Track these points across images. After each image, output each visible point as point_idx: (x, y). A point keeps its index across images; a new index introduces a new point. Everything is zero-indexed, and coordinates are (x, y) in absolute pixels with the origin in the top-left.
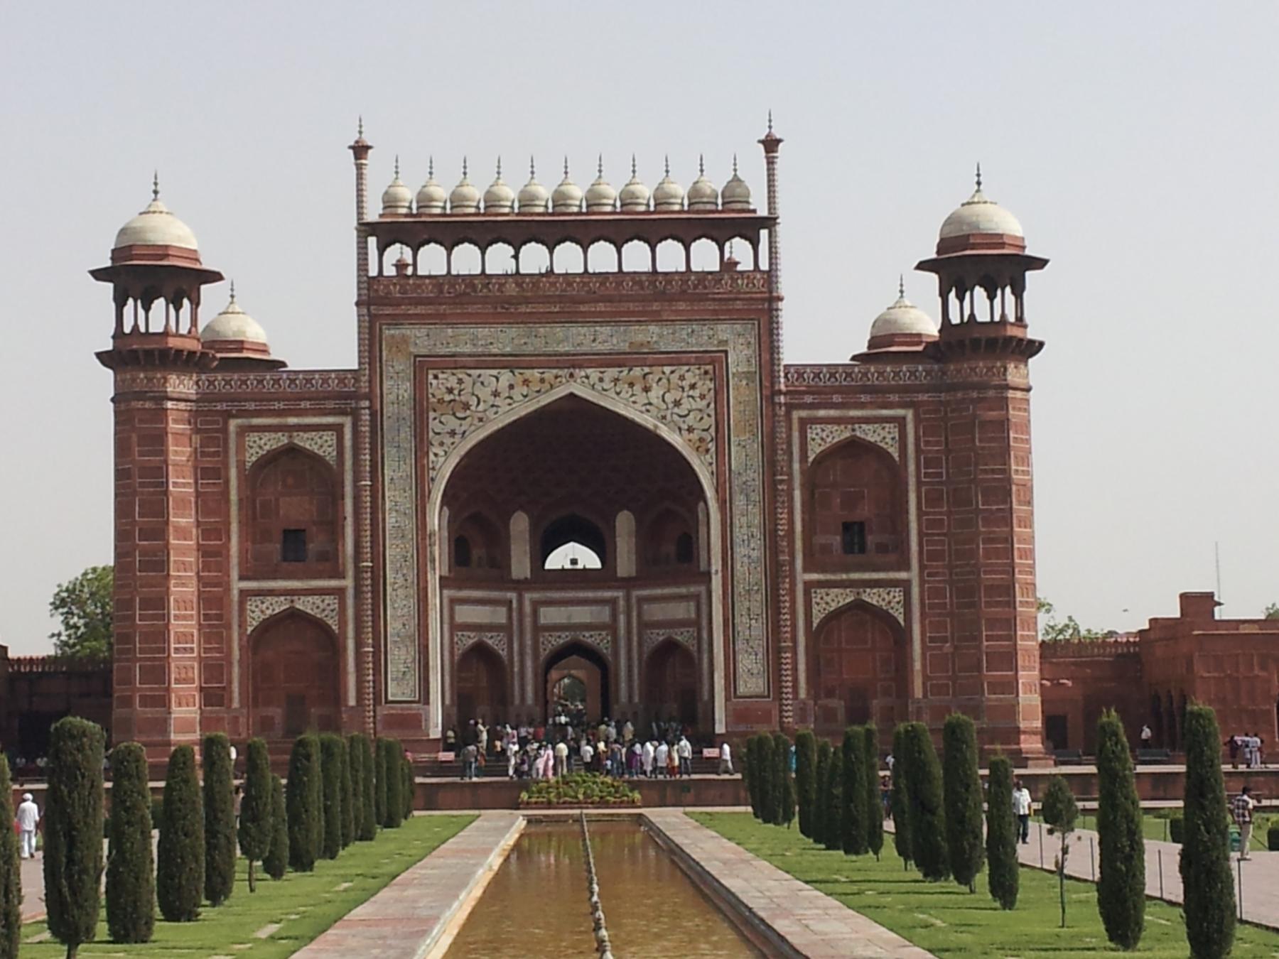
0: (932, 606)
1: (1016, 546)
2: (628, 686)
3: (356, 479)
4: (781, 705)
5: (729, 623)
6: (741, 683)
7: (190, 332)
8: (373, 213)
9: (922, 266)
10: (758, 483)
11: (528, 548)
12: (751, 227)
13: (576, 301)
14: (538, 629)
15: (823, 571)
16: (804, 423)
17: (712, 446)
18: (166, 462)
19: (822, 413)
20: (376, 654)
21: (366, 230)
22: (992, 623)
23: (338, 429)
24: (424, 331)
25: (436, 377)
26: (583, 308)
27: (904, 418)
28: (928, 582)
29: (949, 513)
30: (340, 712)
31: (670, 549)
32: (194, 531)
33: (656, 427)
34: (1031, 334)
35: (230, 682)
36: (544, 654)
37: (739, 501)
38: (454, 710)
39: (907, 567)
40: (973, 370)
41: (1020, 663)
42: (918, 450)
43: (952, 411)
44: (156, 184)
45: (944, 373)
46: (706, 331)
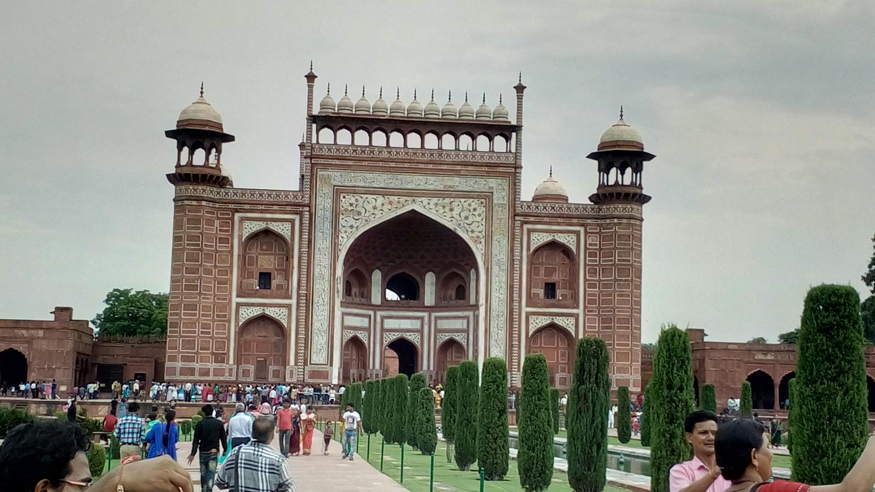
0: (589, 327)
3: (300, 249)
5: (487, 331)
8: (316, 112)
9: (592, 156)
10: (505, 260)
12: (507, 130)
16: (529, 231)
17: (483, 240)
20: (306, 339)
22: (621, 336)
23: (292, 222)
24: (338, 174)
26: (421, 166)
27: (579, 232)
31: (452, 293)
34: (645, 192)
36: (385, 344)
37: (495, 269)
39: (577, 307)
40: (616, 208)
45: (600, 210)
46: (482, 181)
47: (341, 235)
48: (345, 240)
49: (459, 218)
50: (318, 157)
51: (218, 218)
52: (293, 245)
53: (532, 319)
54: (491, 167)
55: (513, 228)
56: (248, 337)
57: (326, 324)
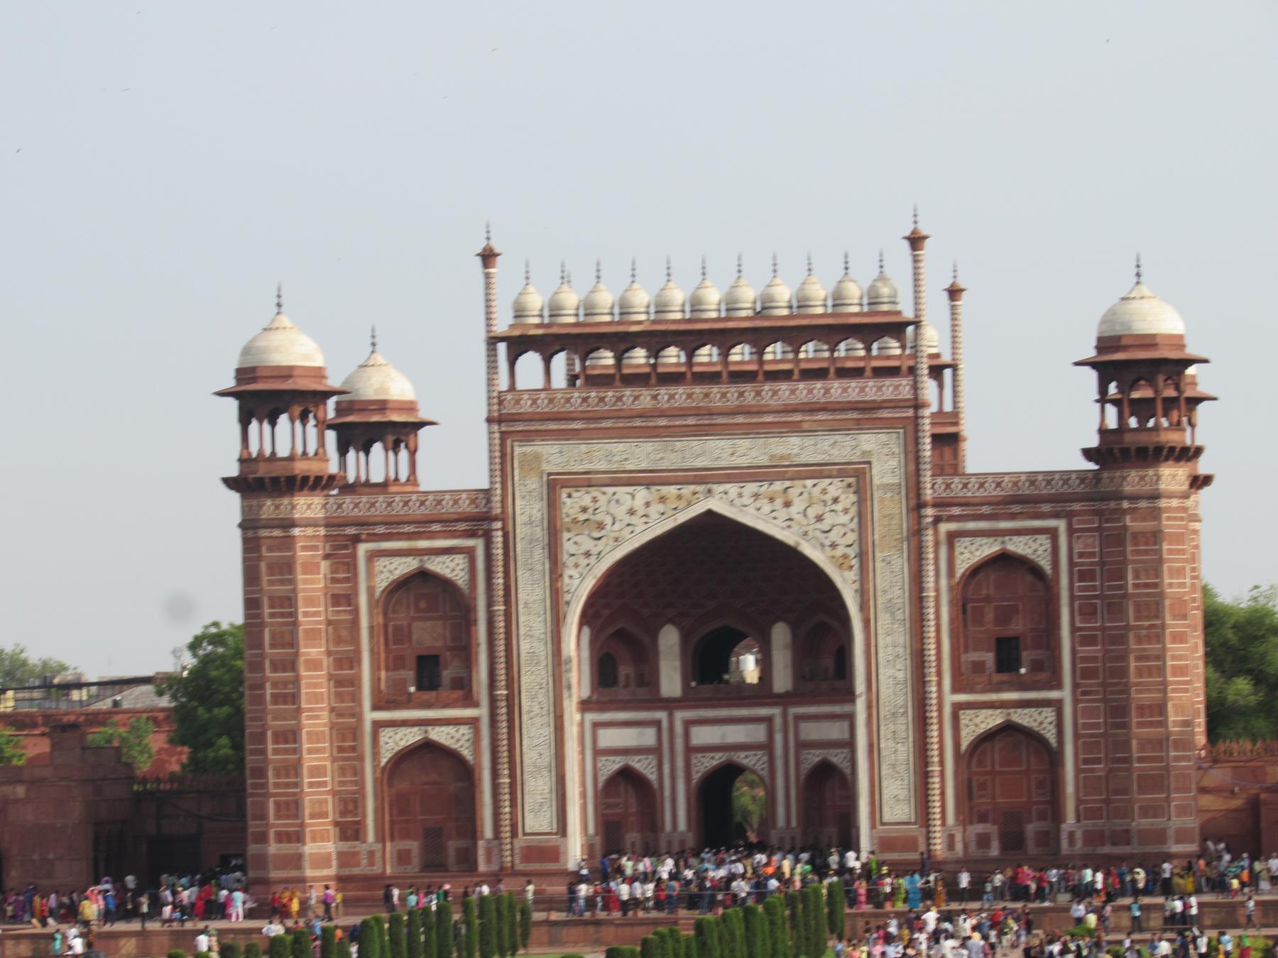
0: (1086, 726)
1: (1169, 663)
3: (490, 603)
4: (929, 832)
6: (886, 809)
7: (316, 454)
8: (503, 324)
11: (678, 663)
13: (711, 413)
14: (690, 750)
15: (971, 690)
16: (952, 537)
17: (855, 562)
18: (294, 591)
19: (971, 525)
20: (513, 785)
21: (493, 341)
22: (1146, 743)
23: (470, 552)
24: (556, 449)
25: (570, 496)
26: (720, 420)
28: (1082, 701)
29: (1103, 629)
30: (475, 846)
31: (828, 662)
32: (324, 659)
33: (798, 544)
35: (364, 816)
36: (696, 777)
37: (883, 621)
38: (598, 841)
39: (1058, 686)
41: (1173, 785)
42: (1072, 564)
43: (1107, 521)
44: (279, 296)
47: (567, 572)
48: (577, 582)
49: (805, 522)
50: (512, 418)
51: (326, 557)
52: (474, 599)
53: (965, 716)
54: (865, 415)
55: (917, 533)
56: (403, 785)
57: (548, 756)
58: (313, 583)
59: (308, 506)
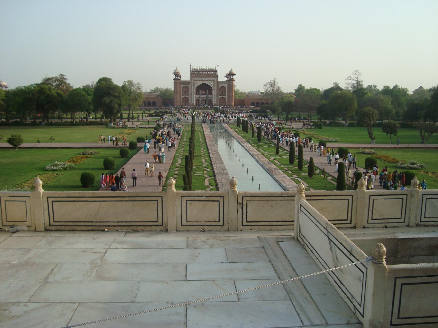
2: (207, 102)
58: (178, 86)
59: (178, 81)
